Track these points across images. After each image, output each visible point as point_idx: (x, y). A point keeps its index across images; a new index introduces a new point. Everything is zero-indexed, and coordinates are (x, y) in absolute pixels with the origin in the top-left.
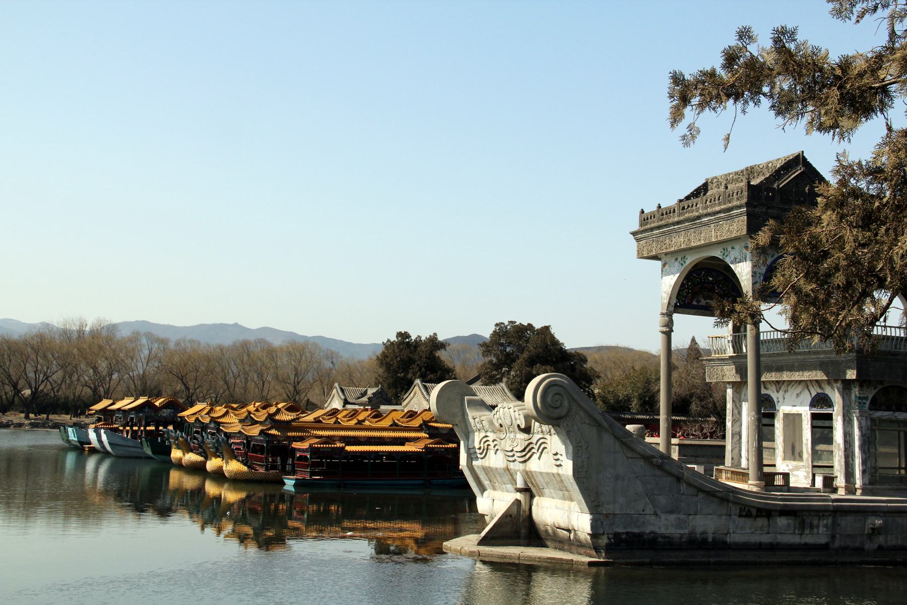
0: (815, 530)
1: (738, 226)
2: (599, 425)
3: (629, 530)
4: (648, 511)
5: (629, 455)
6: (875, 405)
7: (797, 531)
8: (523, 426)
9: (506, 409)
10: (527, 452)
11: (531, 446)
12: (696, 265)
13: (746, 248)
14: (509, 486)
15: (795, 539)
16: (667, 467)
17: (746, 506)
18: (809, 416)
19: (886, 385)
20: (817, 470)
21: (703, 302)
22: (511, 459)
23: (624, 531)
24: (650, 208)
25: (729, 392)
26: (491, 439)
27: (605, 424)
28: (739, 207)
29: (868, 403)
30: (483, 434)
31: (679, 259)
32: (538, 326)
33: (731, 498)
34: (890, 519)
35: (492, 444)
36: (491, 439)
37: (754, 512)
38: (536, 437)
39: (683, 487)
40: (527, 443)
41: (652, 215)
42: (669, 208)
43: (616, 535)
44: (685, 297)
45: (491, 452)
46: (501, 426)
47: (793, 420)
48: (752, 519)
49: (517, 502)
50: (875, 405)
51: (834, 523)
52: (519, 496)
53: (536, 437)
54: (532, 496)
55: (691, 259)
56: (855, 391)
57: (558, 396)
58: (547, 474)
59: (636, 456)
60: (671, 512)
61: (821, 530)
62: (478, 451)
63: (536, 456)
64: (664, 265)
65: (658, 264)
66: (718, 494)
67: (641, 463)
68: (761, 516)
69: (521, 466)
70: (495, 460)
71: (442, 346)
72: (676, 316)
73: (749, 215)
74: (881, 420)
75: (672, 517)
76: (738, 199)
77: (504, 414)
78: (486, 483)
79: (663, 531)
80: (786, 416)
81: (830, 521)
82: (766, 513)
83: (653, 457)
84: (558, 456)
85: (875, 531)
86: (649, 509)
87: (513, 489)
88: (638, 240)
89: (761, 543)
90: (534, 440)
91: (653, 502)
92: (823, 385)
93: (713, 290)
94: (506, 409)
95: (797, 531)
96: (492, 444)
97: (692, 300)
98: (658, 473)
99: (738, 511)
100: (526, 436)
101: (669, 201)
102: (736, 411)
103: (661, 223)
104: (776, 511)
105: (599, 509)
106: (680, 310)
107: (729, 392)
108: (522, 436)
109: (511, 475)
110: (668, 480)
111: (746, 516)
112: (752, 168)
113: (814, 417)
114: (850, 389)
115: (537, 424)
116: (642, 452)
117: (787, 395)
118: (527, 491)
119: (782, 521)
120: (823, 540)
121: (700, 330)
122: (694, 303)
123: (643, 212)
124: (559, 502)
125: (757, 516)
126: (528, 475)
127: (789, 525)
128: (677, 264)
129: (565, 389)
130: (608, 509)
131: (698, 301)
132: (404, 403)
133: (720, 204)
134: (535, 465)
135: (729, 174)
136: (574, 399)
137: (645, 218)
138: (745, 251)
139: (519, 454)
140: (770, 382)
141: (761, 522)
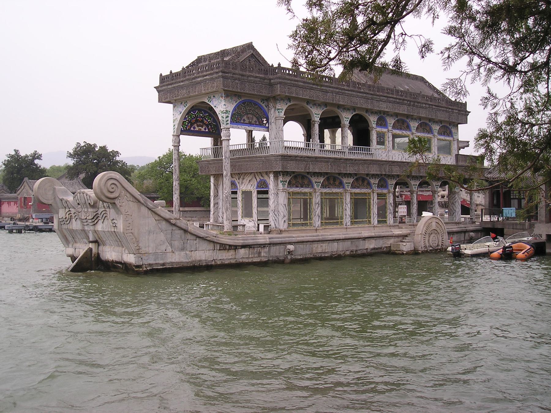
1: (218, 84)
2: (139, 201)
3: (157, 262)
5: (157, 218)
8: (92, 204)
9: (81, 194)
10: (95, 219)
11: (97, 216)
12: (193, 107)
13: (222, 96)
14: (85, 240)
16: (179, 225)
17: (222, 244)
18: (256, 192)
19: (295, 174)
20: (259, 222)
21: (197, 129)
22: (85, 224)
23: (154, 262)
24: (166, 73)
25: (212, 180)
26: (72, 212)
27: (143, 202)
28: (217, 73)
29: (287, 184)
30: (67, 210)
31: (183, 103)
32: (99, 144)
33: (215, 241)
35: (74, 216)
36: (72, 212)
37: (228, 247)
38: (101, 210)
39: (189, 236)
40: (95, 214)
41: (167, 76)
42: (177, 73)
44: (187, 126)
45: (74, 220)
46: (79, 204)
47: (247, 195)
48: (226, 251)
49: (90, 250)
50: (290, 183)
51: (269, 250)
52: (91, 245)
53: (101, 210)
54: (99, 245)
55: (189, 105)
56: (281, 178)
57: (113, 186)
58: (108, 231)
59: (161, 219)
60: (183, 249)
62: (65, 220)
63: (100, 222)
64: (174, 107)
65: (172, 105)
66: (208, 239)
67: (164, 222)
69: (92, 228)
70: (76, 225)
71: (39, 157)
72: (182, 137)
73: (223, 77)
74: (294, 193)
75: (183, 253)
76: (217, 68)
77: (80, 197)
78: (70, 239)
79: (177, 260)
80: (243, 192)
82: (235, 247)
84: (114, 221)
85: (290, 252)
86: (169, 249)
87: (87, 242)
88: (159, 91)
90: (99, 212)
91: (171, 245)
92: (263, 175)
93: (202, 121)
94: (81, 194)
95: (250, 256)
96: (74, 216)
97: (191, 127)
98: (174, 228)
100: (95, 210)
101: (177, 69)
102: (216, 191)
103: (172, 82)
104: (239, 246)
105: (140, 251)
106: (184, 133)
107: (212, 180)
108: (90, 210)
109: (86, 233)
110: (178, 232)
112: (224, 50)
113: (259, 192)
114: (278, 177)
115: (101, 202)
116: (164, 217)
117: (245, 180)
118: (95, 242)
119: (242, 251)
121: (196, 146)
122: (192, 129)
123: (161, 75)
124: (117, 249)
125: (229, 249)
126: (95, 232)
127: (245, 253)
128: (182, 106)
129: (117, 180)
130: (143, 250)
131: (194, 128)
132: (19, 192)
133: (206, 71)
134: (100, 227)
135: (211, 54)
136: (123, 187)
137: (163, 79)
138: (221, 99)
139: (90, 221)
140: (234, 174)
141: (232, 252)
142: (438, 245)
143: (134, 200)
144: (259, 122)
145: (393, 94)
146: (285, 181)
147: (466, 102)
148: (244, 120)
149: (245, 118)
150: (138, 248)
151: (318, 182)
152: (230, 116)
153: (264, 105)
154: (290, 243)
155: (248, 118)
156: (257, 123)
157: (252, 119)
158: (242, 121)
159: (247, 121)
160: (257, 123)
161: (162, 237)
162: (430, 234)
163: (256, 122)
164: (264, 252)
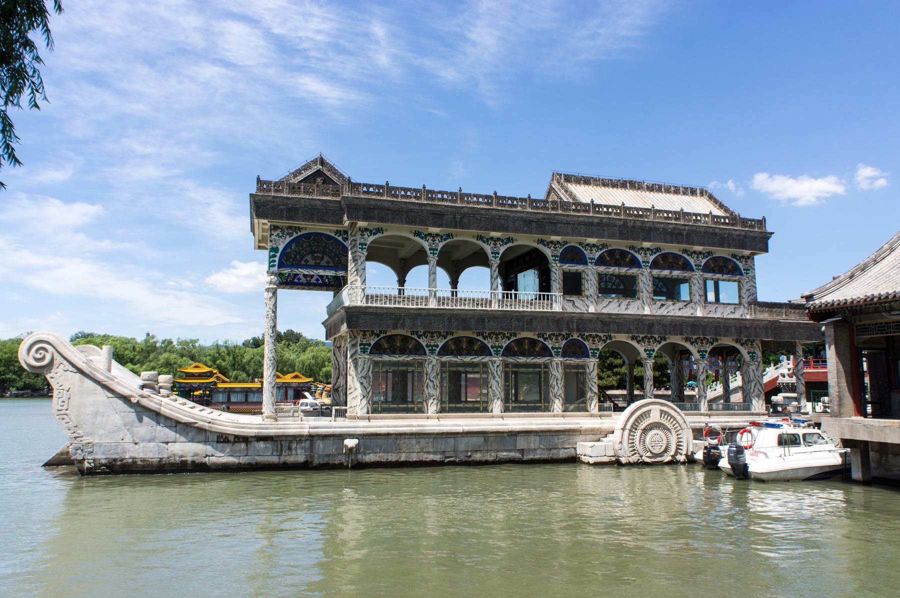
0: (294, 452)
4: (126, 440)
5: (110, 395)
6: (378, 349)
7: (275, 453)
15: (275, 459)
17: (222, 434)
34: (368, 441)
43: (95, 460)
60: (150, 441)
61: (299, 451)
68: (238, 442)
81: (308, 444)
83: (132, 396)
89: (249, 464)
99: (216, 438)
111: (224, 442)
120: (301, 459)
125: (235, 442)
127: (266, 448)
142: (666, 451)
143: (73, 369)
144: (334, 263)
145: (588, 211)
146: (366, 344)
147: (764, 219)
148: (307, 261)
149: (309, 257)
150: (75, 435)
151: (432, 346)
152: (278, 255)
153: (340, 239)
154: (351, 436)
155: (314, 258)
156: (331, 264)
157: (322, 258)
158: (303, 263)
159: (312, 262)
160: (331, 264)
161: (117, 419)
162: (645, 431)
163: (328, 262)
164: (302, 448)
